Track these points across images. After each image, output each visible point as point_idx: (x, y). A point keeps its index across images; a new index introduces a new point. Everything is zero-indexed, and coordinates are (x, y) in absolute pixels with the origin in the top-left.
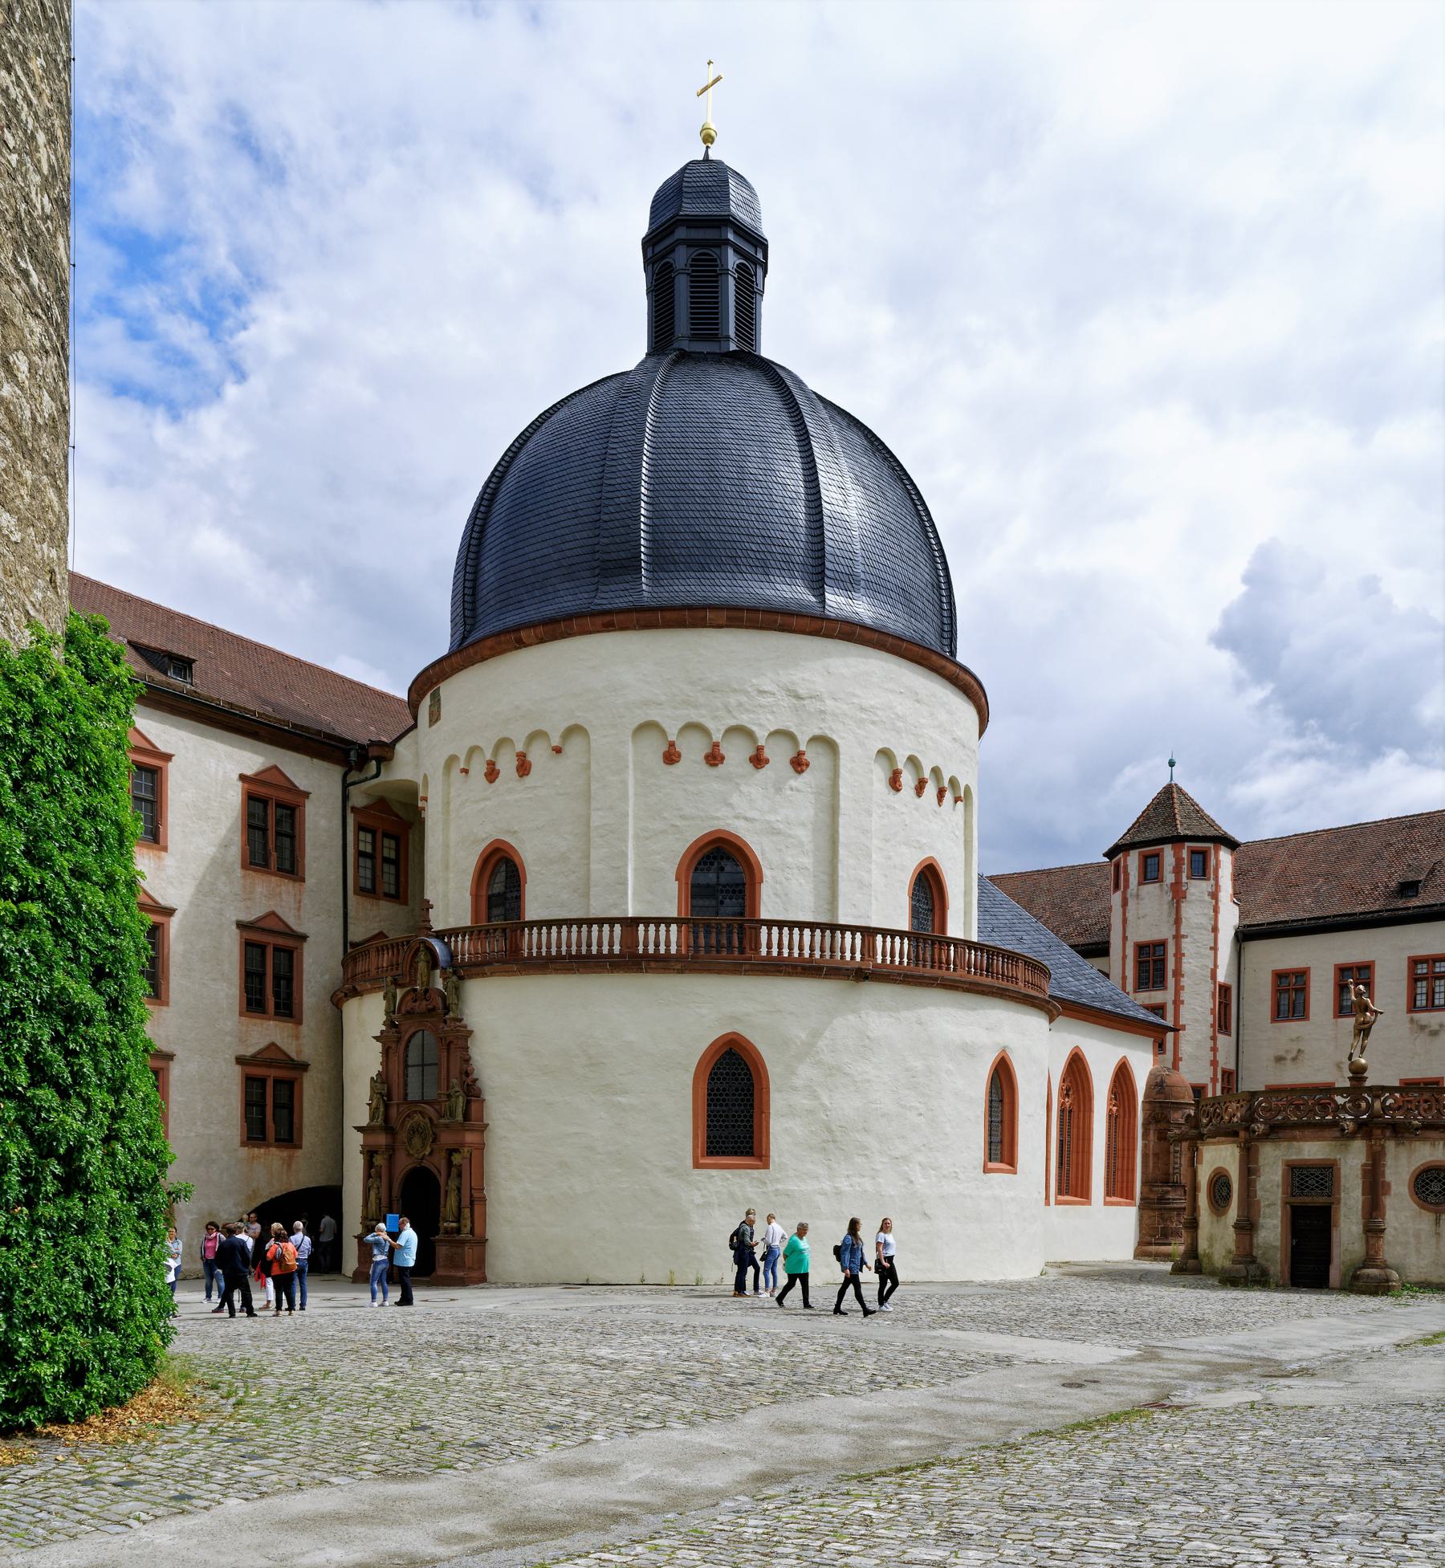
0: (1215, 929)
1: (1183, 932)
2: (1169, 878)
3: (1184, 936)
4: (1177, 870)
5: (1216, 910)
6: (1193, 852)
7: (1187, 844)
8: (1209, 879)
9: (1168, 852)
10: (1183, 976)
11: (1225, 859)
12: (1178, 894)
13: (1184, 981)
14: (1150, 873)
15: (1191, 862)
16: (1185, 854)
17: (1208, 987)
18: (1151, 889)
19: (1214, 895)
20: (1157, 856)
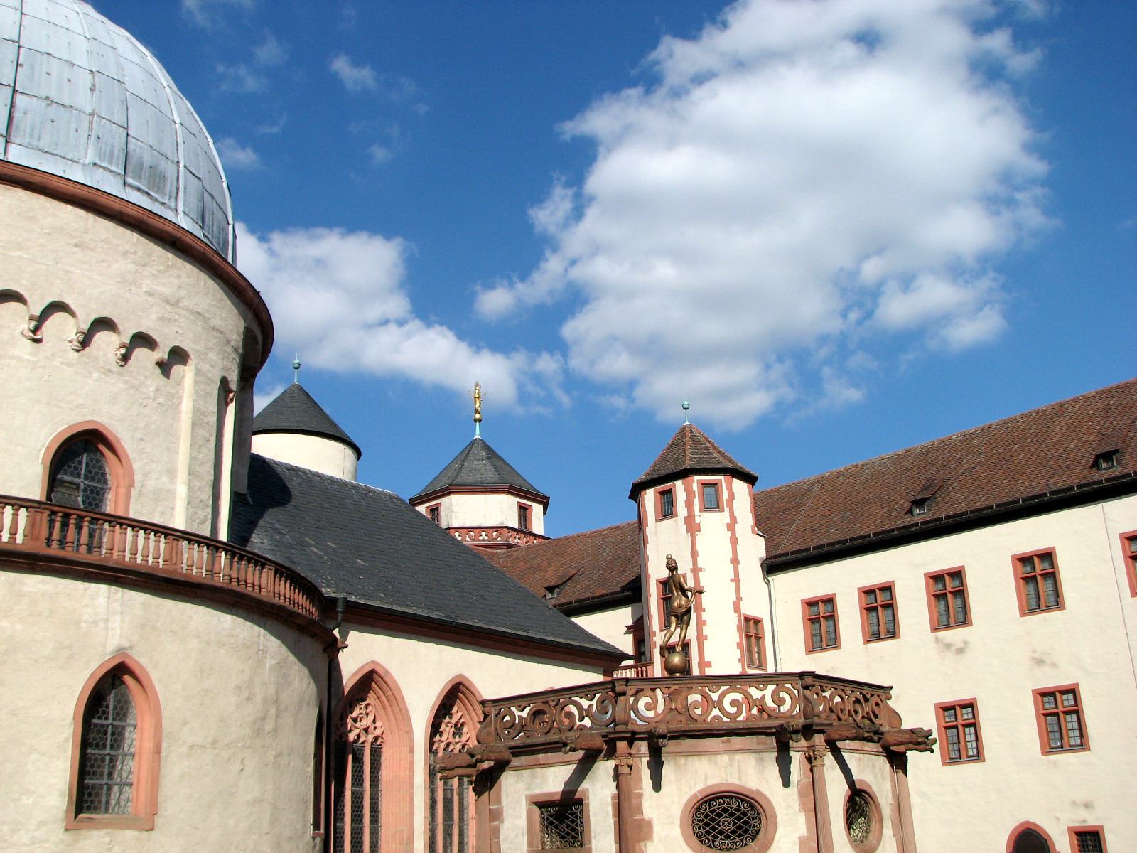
0: (735, 561)
1: (700, 565)
2: (682, 510)
3: (701, 570)
4: (689, 504)
5: (734, 541)
6: (705, 484)
7: (697, 478)
8: (723, 511)
9: (679, 485)
10: (704, 610)
11: (740, 487)
12: (692, 527)
13: (705, 616)
14: (667, 511)
15: (703, 495)
16: (695, 487)
17: (733, 620)
18: (668, 523)
19: (731, 527)
20: (669, 492)
